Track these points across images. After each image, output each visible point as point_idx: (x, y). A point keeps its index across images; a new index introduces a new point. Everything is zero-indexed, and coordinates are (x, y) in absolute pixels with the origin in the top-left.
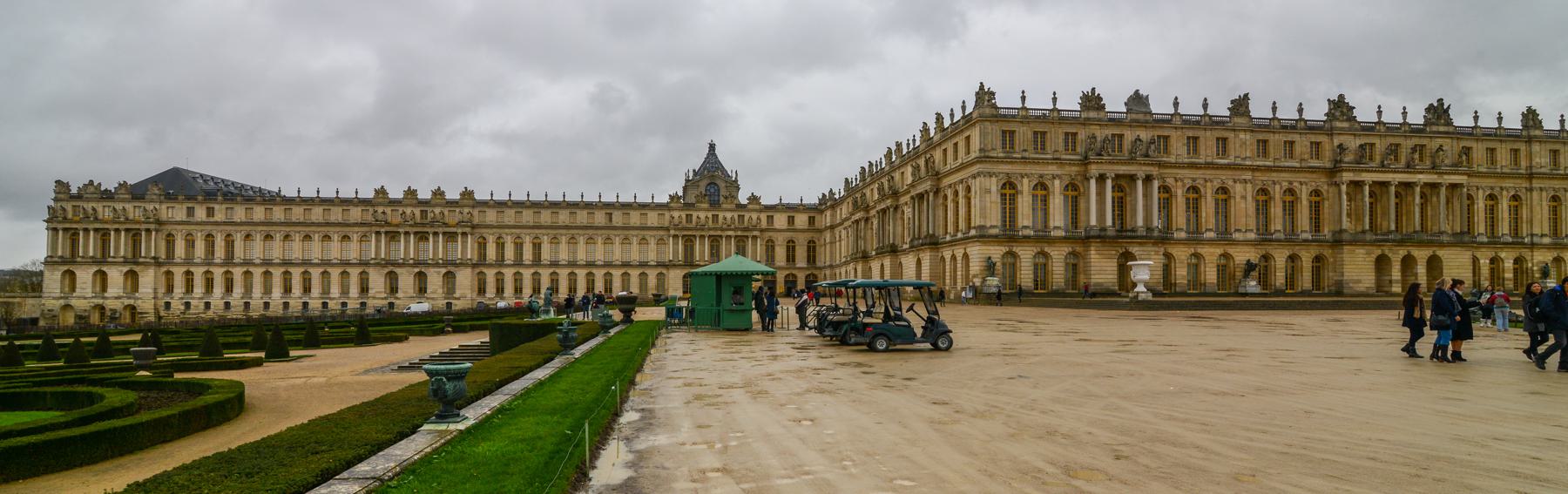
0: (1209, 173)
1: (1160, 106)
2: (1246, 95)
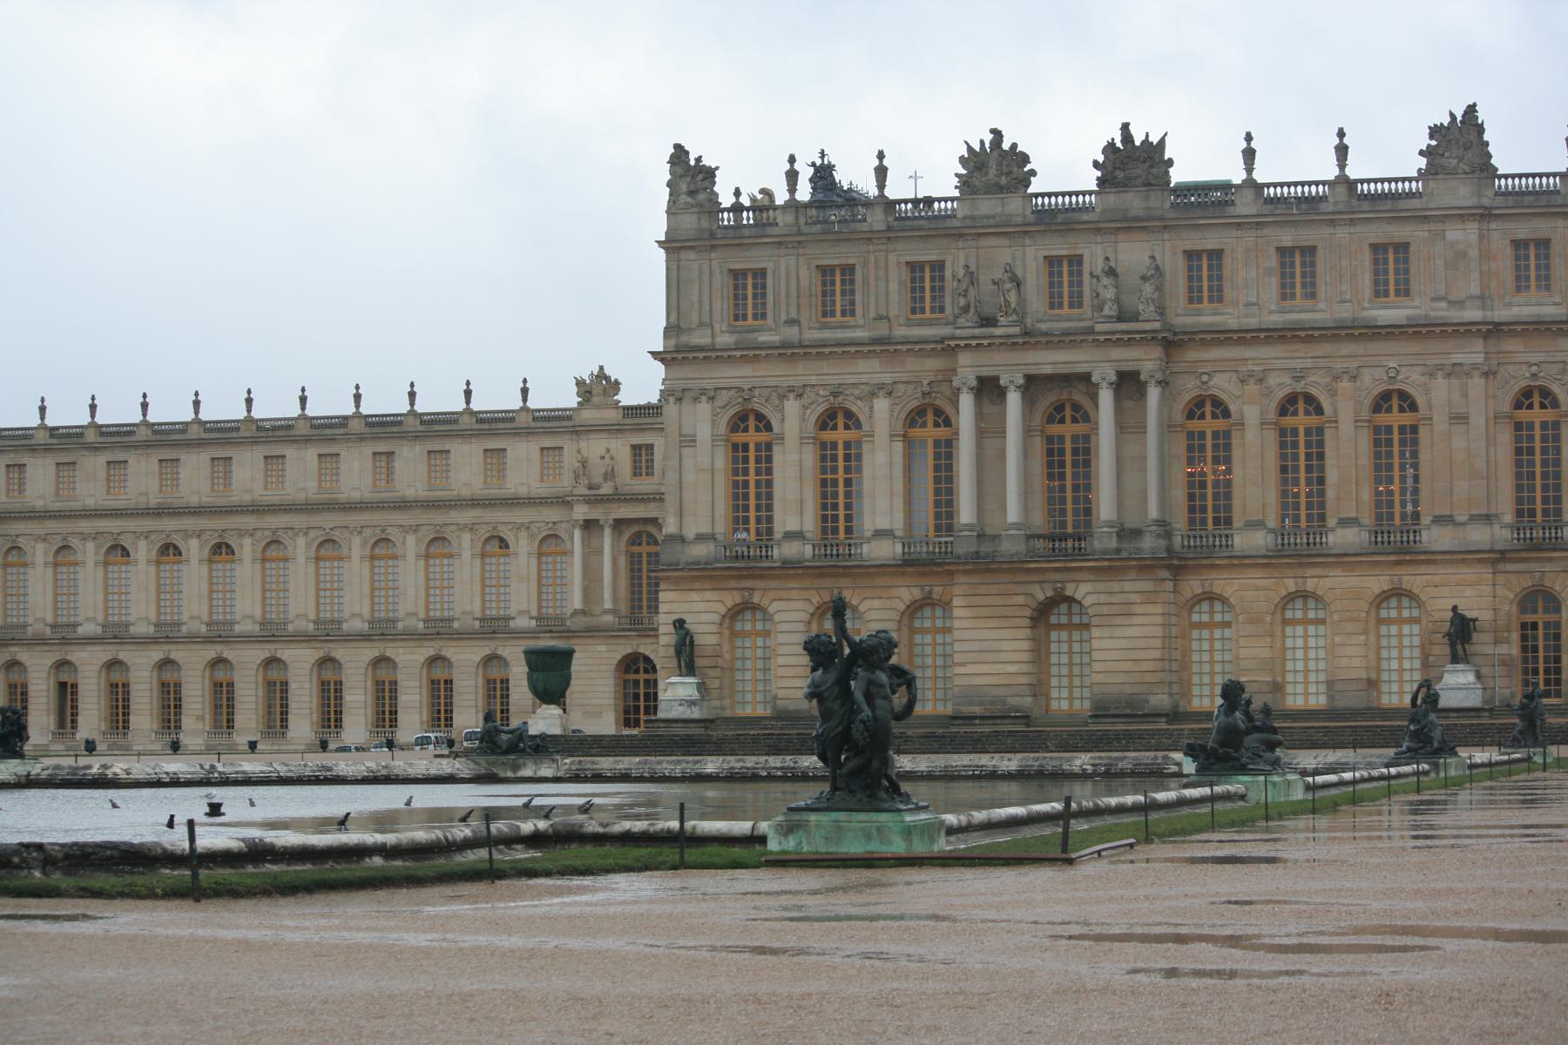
0: (1345, 353)
1: (1197, 160)
2: (1471, 110)
